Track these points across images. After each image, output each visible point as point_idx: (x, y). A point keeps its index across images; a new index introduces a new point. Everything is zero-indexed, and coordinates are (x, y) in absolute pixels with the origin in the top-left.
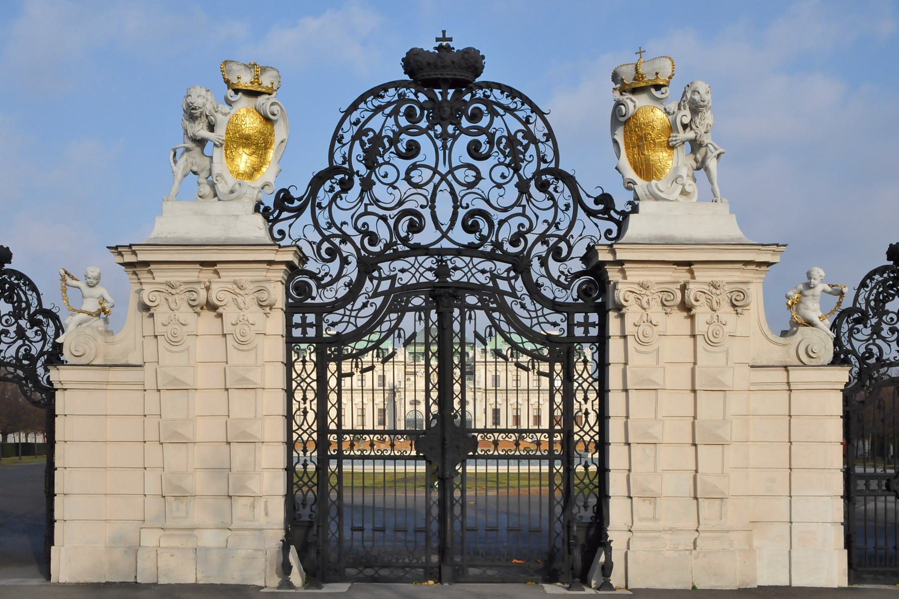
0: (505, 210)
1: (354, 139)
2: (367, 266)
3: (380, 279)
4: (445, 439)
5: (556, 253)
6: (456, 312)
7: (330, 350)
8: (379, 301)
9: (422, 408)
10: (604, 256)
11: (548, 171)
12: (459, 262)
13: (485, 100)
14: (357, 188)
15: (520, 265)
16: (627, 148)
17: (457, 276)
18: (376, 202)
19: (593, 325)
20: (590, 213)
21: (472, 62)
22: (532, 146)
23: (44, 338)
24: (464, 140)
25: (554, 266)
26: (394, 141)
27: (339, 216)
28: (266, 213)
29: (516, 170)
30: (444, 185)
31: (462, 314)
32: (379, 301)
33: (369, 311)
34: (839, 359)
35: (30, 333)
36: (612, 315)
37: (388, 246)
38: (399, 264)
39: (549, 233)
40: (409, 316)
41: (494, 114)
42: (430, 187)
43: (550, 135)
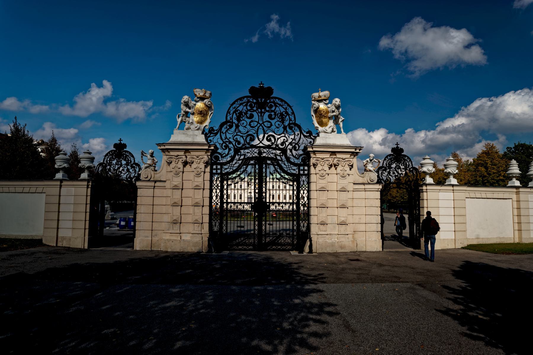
0: (279, 135)
1: (233, 113)
2: (237, 151)
3: (241, 155)
4: (260, 205)
5: (294, 148)
6: (264, 166)
7: (224, 177)
8: (240, 162)
9: (253, 194)
10: (310, 149)
11: (292, 124)
12: (265, 150)
13: (274, 102)
14: (234, 127)
15: (284, 151)
16: (316, 117)
17: (264, 155)
18: (240, 132)
19: (306, 170)
20: (305, 136)
21: (270, 90)
22: (288, 116)
23: (135, 172)
24: (267, 114)
25: (294, 152)
26: (246, 113)
27: (228, 136)
28: (206, 135)
29: (283, 123)
30: (261, 127)
31: (266, 166)
32: (240, 162)
33: (237, 165)
34: (379, 182)
35: (131, 170)
36: (312, 168)
37: (243, 145)
38: (246, 151)
40: (249, 167)
41: (276, 106)
42: (256, 128)
43: (293, 113)
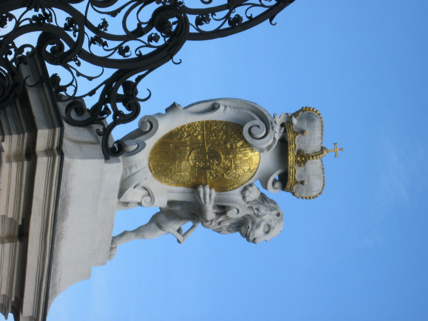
11: (183, 24)
39: (86, 30)
43: (236, 26)
